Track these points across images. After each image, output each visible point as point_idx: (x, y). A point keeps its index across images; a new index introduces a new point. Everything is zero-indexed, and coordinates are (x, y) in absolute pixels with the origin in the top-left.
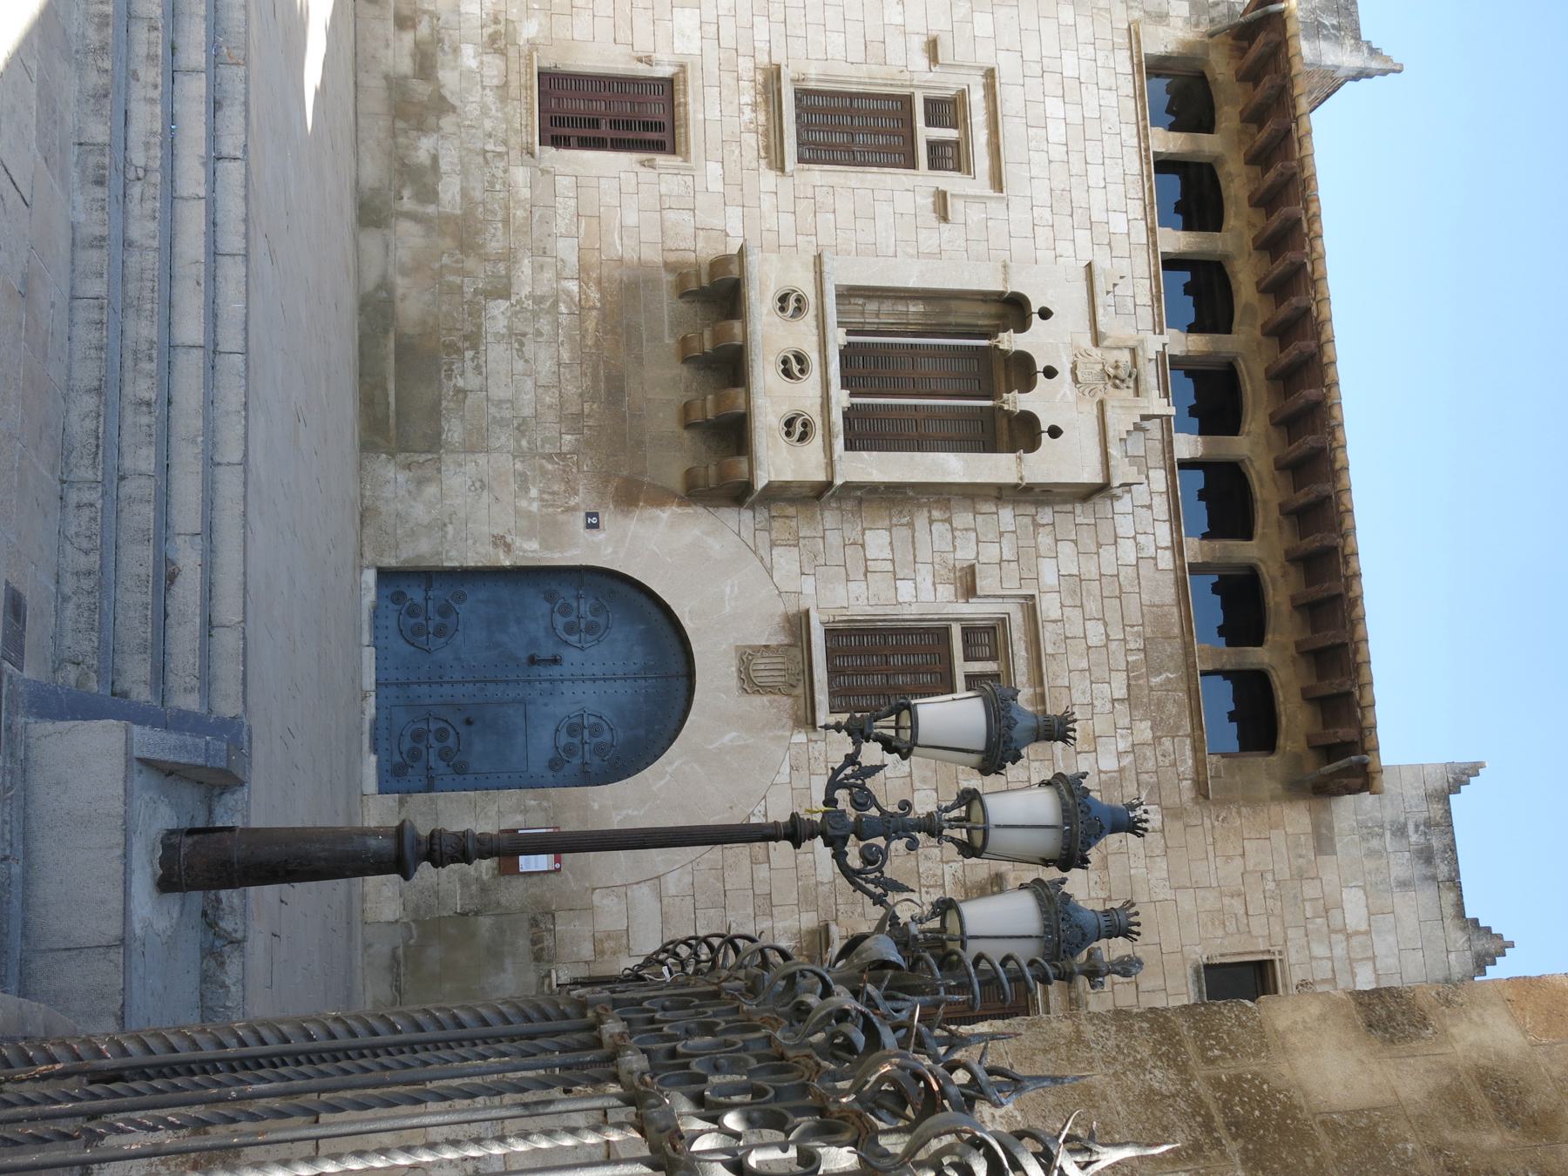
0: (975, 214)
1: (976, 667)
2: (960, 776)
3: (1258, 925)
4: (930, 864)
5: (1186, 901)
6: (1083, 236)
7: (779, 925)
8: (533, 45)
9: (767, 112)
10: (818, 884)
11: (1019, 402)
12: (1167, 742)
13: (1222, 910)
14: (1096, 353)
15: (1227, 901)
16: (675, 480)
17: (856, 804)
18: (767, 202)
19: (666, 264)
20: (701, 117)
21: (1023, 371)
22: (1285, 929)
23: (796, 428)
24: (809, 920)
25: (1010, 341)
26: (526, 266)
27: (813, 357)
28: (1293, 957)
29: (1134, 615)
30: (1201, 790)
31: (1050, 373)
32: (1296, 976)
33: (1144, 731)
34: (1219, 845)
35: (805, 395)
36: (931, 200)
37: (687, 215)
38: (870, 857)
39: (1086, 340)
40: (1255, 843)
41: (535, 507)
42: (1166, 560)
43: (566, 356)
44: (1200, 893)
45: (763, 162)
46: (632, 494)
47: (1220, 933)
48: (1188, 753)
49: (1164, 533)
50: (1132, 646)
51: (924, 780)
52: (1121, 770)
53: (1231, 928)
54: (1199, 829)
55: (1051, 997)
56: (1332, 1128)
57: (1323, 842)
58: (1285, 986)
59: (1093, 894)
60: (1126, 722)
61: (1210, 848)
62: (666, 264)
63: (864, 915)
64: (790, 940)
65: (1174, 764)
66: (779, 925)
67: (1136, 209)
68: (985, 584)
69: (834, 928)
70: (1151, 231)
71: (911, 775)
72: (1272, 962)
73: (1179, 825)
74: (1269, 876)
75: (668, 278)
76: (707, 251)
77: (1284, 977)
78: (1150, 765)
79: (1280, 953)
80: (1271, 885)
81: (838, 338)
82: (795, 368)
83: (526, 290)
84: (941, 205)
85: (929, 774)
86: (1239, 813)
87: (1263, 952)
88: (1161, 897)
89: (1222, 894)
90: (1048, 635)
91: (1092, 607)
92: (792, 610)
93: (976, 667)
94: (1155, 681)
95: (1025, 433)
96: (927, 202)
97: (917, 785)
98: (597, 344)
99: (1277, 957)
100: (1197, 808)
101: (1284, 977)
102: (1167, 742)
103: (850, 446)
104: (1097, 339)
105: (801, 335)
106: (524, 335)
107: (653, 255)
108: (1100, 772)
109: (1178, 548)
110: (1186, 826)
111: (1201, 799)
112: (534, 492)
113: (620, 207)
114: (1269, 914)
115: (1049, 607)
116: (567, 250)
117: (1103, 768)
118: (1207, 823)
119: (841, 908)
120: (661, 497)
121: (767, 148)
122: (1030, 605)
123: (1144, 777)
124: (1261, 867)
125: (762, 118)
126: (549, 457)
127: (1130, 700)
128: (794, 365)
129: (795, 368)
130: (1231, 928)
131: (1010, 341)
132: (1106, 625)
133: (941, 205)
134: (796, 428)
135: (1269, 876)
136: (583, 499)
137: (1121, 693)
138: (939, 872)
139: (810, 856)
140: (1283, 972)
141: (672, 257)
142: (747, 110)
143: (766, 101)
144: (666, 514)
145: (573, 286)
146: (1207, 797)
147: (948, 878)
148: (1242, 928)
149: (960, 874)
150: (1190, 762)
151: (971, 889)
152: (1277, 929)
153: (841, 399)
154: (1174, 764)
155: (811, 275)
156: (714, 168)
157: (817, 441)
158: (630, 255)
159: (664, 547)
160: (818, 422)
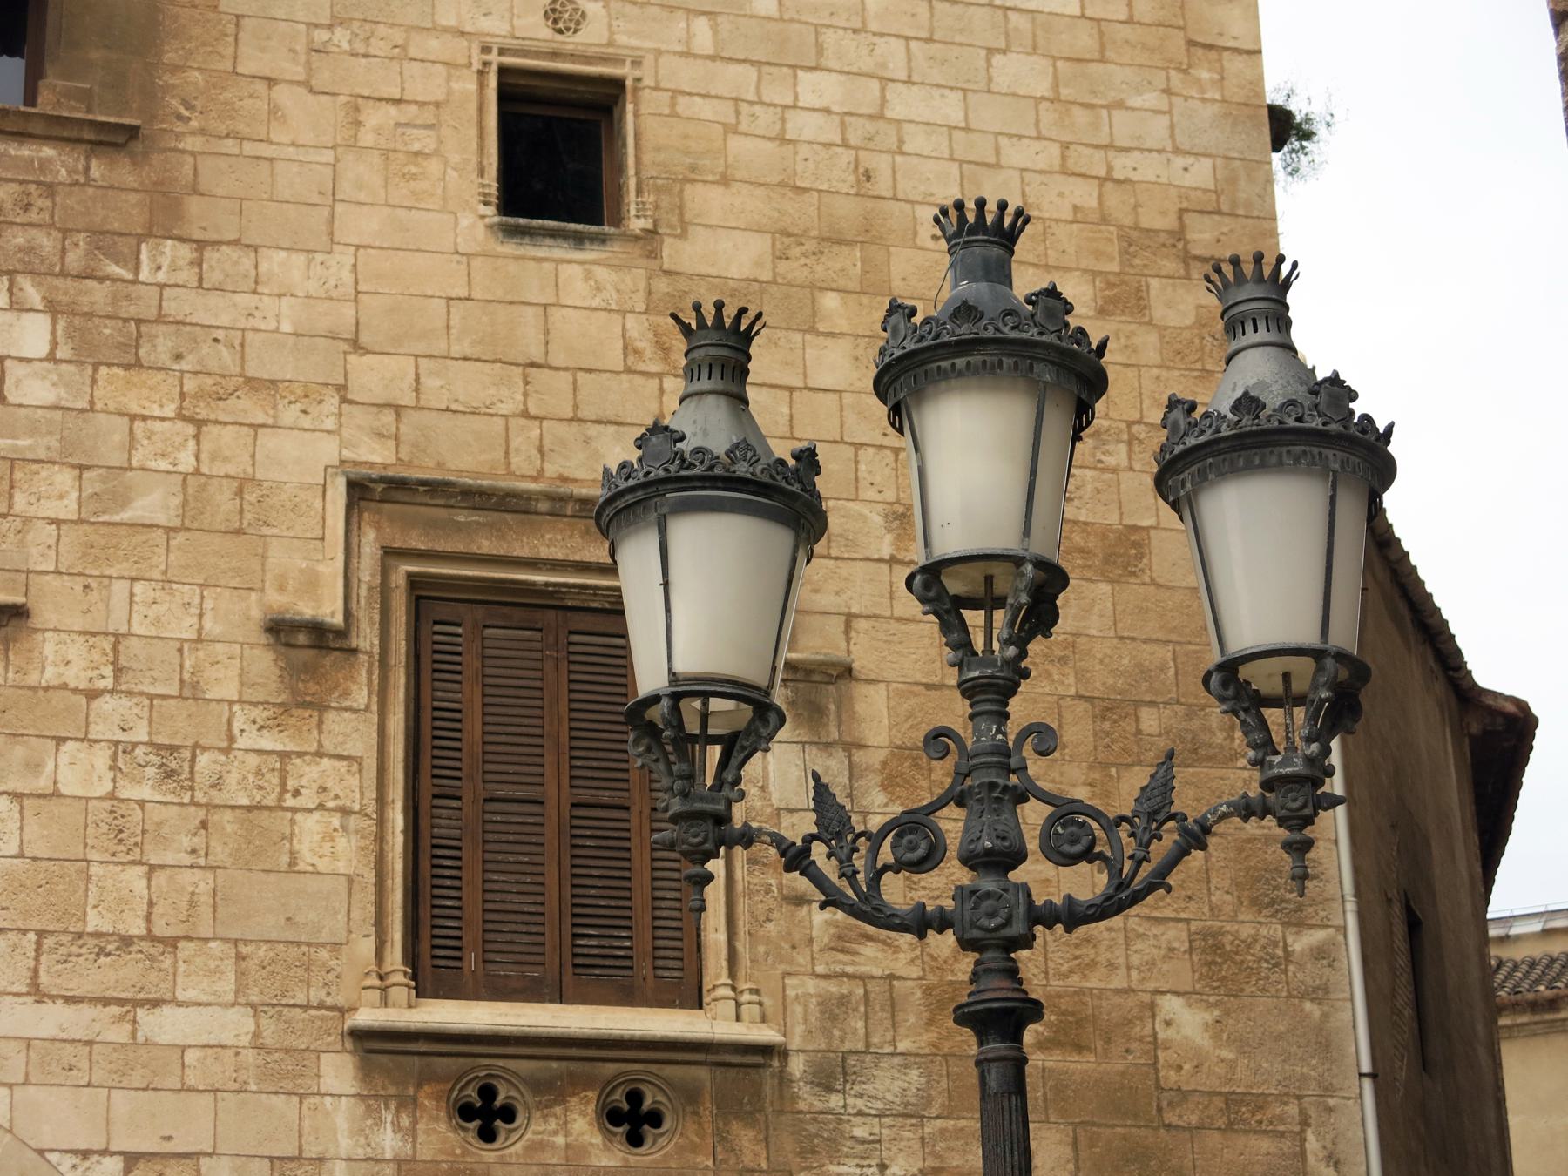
2: (33, 679)
3: (425, 84)
4: (232, 779)
5: (361, 224)
7: (345, 1144)
10: (258, 1046)
13: (386, 154)
15: (367, 138)
17: (927, 861)
22: (436, 30)
24: (338, 1072)
28: (495, 26)
30: (117, 139)
32: (538, 31)
34: (243, 129)
38: (1072, 835)
40: (244, 49)
44: (346, 189)
47: (434, 166)
48: (26, 151)
51: (34, 767)
52: (52, 308)
53: (423, 140)
54: (206, 165)
55: (545, 553)
58: (555, 55)
59: (330, 424)
61: (248, 148)
63: (335, 946)
64: (379, 1122)
65: (50, 189)
66: (345, 1144)
69: (367, 1017)
71: (17, 796)
72: (503, 71)
73: (194, 205)
74: (321, 36)
77: (537, 54)
78: (46, 242)
79: (486, 50)
80: (341, 37)
85: (19, 752)
86: (175, 69)
87: (482, 86)
88: (348, 277)
89: (353, 145)
97: (43, 783)
99: (494, 58)
100: (156, 158)
101: (537, 54)
108: (51, 357)
110: (195, 191)
111: (138, 147)
114: (402, 54)
117: (44, 350)
118: (189, 143)
119: (316, 995)
123: (74, 259)
124: (300, 47)
130: (423, 140)
135: (321, 36)
138: (253, 760)
139: (191, 1057)
140: (524, 53)
146: (133, 132)
147: (268, 742)
148: (428, 116)
149: (259, 714)
150: (48, 151)
151: (294, 692)
152: (434, 46)
154: (50, 189)
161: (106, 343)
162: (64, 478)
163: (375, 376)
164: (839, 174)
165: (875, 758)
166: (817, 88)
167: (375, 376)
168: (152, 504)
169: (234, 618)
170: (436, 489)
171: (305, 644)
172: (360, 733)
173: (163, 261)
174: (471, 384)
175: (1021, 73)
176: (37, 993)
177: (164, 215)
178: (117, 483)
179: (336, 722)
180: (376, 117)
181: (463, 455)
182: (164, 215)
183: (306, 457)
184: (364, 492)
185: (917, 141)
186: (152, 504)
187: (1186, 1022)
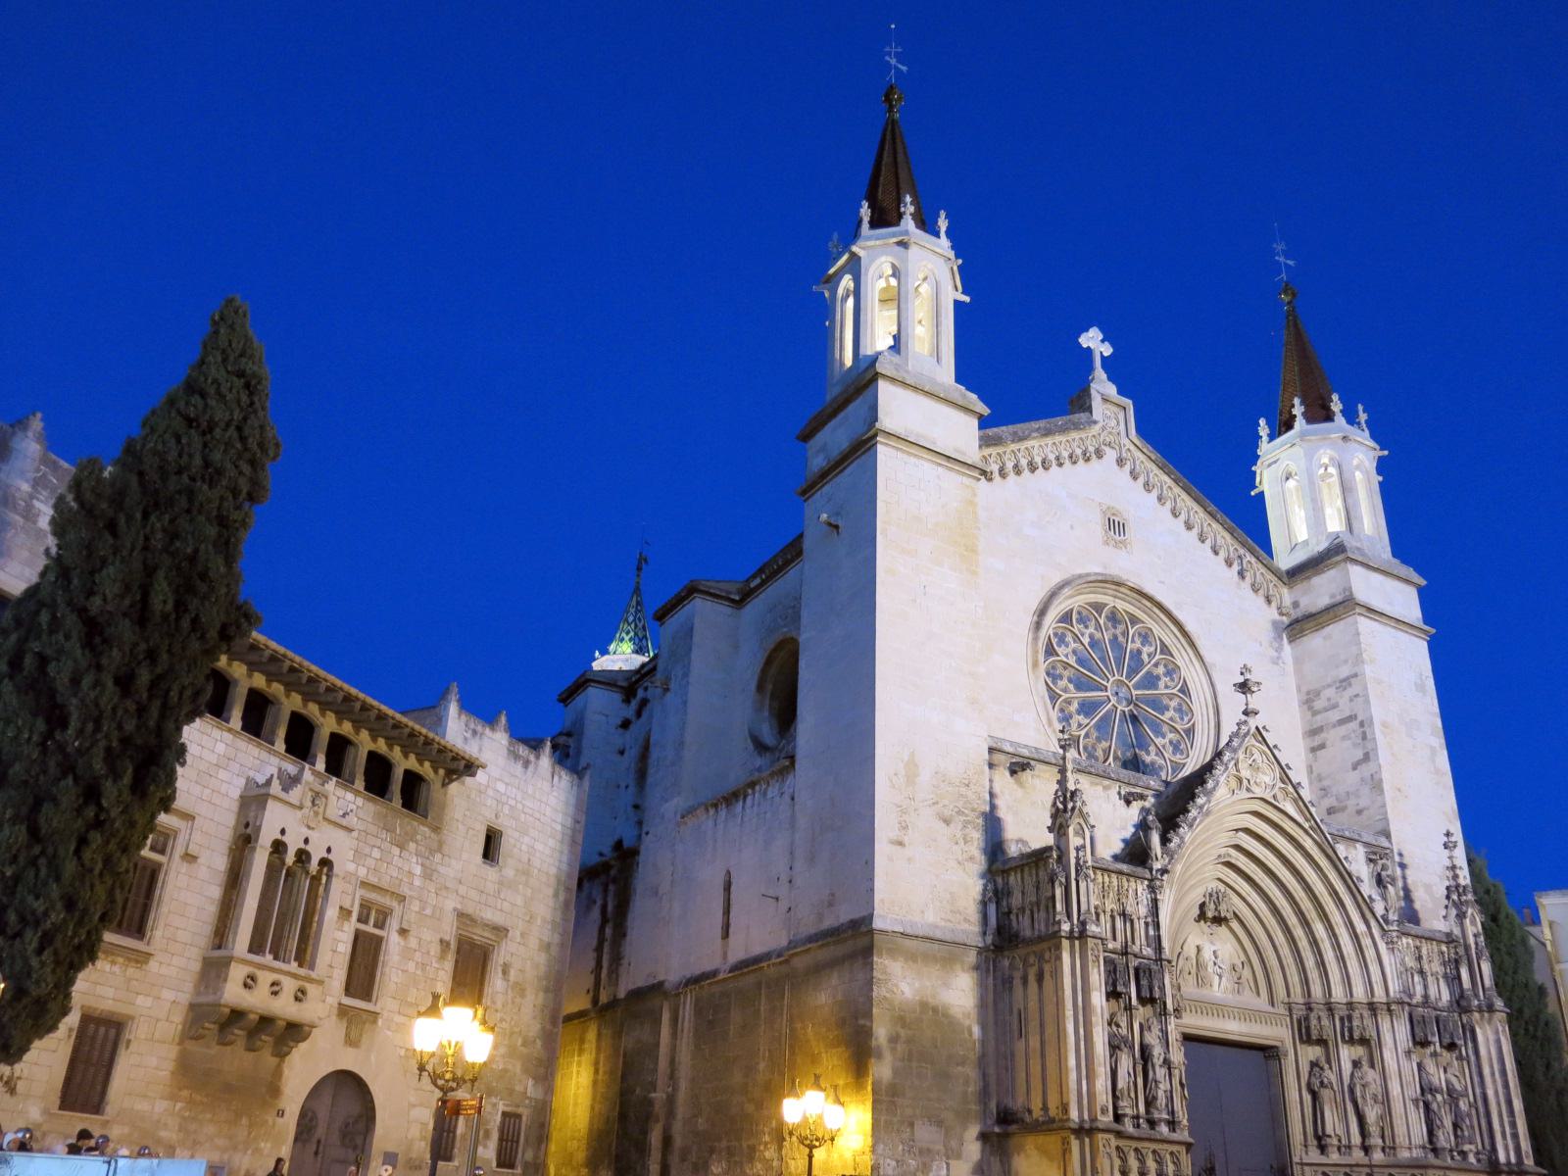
0: (197, 837)
1: (372, 921)
6: (222, 775)
8: (46, 1112)
9: (118, 955)
12: (419, 837)
14: (305, 811)
16: (273, 1061)
18: (164, 970)
19: (179, 1044)
20: (110, 1002)
21: (303, 856)
23: (300, 996)
26: (163, 1134)
27: (275, 977)
29: (373, 829)
30: (436, 829)
31: (306, 841)
33: (412, 846)
35: (289, 985)
36: (185, 864)
37: (159, 1025)
38: (817, 1140)
39: (299, 814)
41: (269, 1145)
42: (360, 801)
43: (209, 1116)
45: (144, 966)
46: (275, 1091)
49: (350, 796)
50: (384, 836)
56: (894, 1078)
57: (463, 783)
60: (407, 854)
62: (179, 1044)
67: (217, 733)
68: (347, 905)
70: (230, 730)
75: (191, 1046)
76: (178, 1018)
81: (269, 957)
82: (276, 988)
83: (174, 1136)
84: (189, 858)
90: (374, 880)
91: (367, 850)
92: (335, 1011)
93: (372, 921)
94: (398, 832)
96: (184, 867)
98: (207, 1096)
102: (419, 837)
103: (312, 967)
104: (301, 808)
105: (265, 978)
106: (194, 1141)
107: (172, 1052)
109: (357, 793)
112: (262, 1145)
115: (362, 872)
116: (161, 1106)
120: (278, 1073)
121: (137, 962)
122: (364, 884)
125: (121, 960)
126: (250, 1133)
127: (402, 847)
128: (275, 989)
129: (276, 988)
132: (374, 846)
133: (189, 858)
134: (300, 996)
136: (270, 1118)
137: (396, 851)
141: (177, 1040)
142: (116, 969)
143: (113, 954)
144: (286, 1072)
145: (179, 1105)
150: (426, 829)
153: (293, 966)
155: (241, 966)
156: (140, 1000)
157: (309, 987)
158: (169, 1066)
160: (300, 983)
161: (428, 874)
162: (418, 902)
164: (525, 858)
165: (511, 983)
166: (526, 839)
167: (462, 890)
168: (428, 912)
170: (468, 915)
173: (438, 856)
174: (473, 894)
176: (399, 1013)
178: (424, 903)
179: (446, 963)
180: (471, 831)
181: (470, 911)
182: (440, 849)
183: (450, 904)
184: (461, 915)
185: (538, 854)
186: (428, 912)
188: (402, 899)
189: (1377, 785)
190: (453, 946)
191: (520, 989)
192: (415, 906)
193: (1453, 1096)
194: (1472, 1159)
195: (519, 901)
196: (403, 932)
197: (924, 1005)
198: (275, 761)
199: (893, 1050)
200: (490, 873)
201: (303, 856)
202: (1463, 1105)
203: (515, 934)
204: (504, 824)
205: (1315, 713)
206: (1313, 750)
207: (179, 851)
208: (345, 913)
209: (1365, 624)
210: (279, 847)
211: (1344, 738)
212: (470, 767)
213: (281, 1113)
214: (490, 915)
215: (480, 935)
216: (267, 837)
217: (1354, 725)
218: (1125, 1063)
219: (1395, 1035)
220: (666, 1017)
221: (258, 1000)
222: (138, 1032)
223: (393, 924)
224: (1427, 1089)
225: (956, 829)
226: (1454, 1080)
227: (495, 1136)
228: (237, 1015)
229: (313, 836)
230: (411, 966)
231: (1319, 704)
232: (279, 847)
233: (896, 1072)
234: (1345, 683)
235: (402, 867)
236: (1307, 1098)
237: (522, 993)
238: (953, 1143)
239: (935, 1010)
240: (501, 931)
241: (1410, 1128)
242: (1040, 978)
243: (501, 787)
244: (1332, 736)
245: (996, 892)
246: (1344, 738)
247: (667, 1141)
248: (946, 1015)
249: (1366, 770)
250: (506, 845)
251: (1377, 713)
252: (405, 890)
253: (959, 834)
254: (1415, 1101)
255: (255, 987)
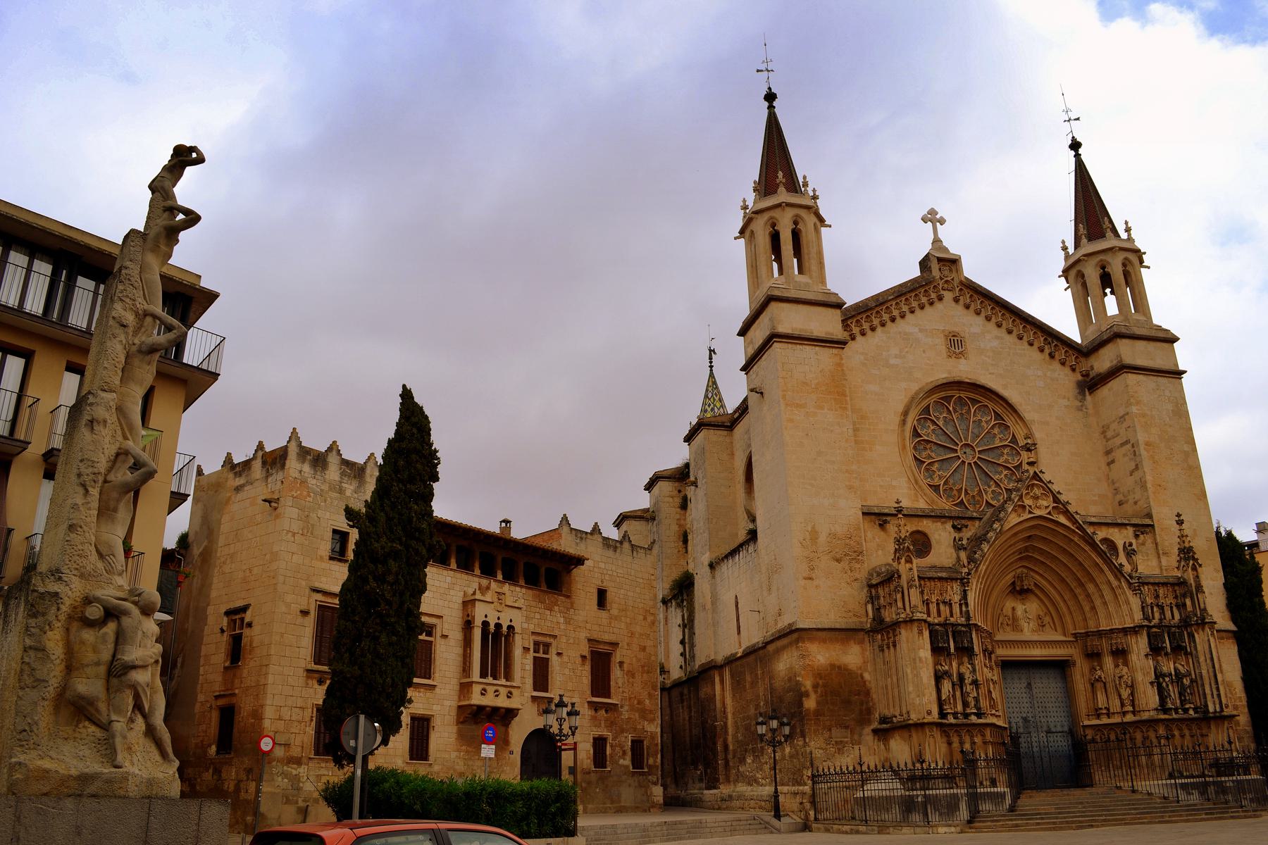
0: (446, 626)
6: (452, 592)
11: (505, 629)
21: (498, 626)
25: (492, 627)
29: (533, 604)
30: (568, 597)
33: (556, 608)
35: (503, 691)
42: (524, 590)
49: (518, 589)
67: (445, 572)
76: (454, 713)
90: (538, 630)
95: (510, 628)
96: (443, 641)
105: (491, 689)
107: (454, 729)
109: (521, 587)
113: (443, 738)
115: (532, 628)
116: (454, 755)
120: (507, 733)
131: (492, 627)
137: (548, 612)
153: (503, 682)
158: (455, 736)
159: (519, 733)
161: (568, 621)
163: (588, 626)
167: (588, 626)
169: (578, 655)
171: (584, 657)
172: (588, 667)
175: (638, 590)
177: (572, 607)
181: (595, 636)
182: (572, 607)
183: (583, 635)
184: (589, 640)
187: (647, 702)
188: (555, 637)
189: (1143, 485)
190: (589, 657)
191: (631, 674)
192: (564, 640)
193: (1179, 676)
194: (1191, 712)
195: (623, 626)
196: (559, 654)
197: (832, 666)
198: (476, 579)
199: (816, 692)
200: (603, 614)
201: (498, 626)
202: (1186, 682)
203: (623, 644)
204: (607, 585)
205: (1108, 440)
206: (1109, 464)
207: (439, 635)
208: (526, 649)
209: (1131, 378)
210: (485, 624)
211: (1125, 455)
212: (579, 561)
213: (511, 753)
214: (607, 637)
215: (603, 648)
216: (478, 622)
217: (1129, 446)
218: (946, 686)
219: (1140, 646)
220: (717, 679)
221: (488, 701)
222: (437, 722)
223: (553, 651)
224: (1159, 675)
225: (845, 564)
226: (1180, 667)
227: (629, 753)
228: (481, 708)
229: (502, 615)
230: (567, 671)
231: (1109, 434)
232: (485, 624)
233: (818, 703)
234: (1122, 418)
235: (551, 620)
236: (1088, 687)
237: (633, 676)
238: (856, 737)
239: (839, 667)
240: (615, 645)
241: (1149, 698)
242: (895, 646)
243: (602, 565)
244: (1118, 454)
245: (871, 597)
246: (1125, 455)
247: (726, 747)
248: (846, 669)
249: (1137, 475)
250: (609, 596)
251: (1141, 437)
252: (556, 633)
253: (847, 568)
254: (1152, 683)
255: (487, 696)
